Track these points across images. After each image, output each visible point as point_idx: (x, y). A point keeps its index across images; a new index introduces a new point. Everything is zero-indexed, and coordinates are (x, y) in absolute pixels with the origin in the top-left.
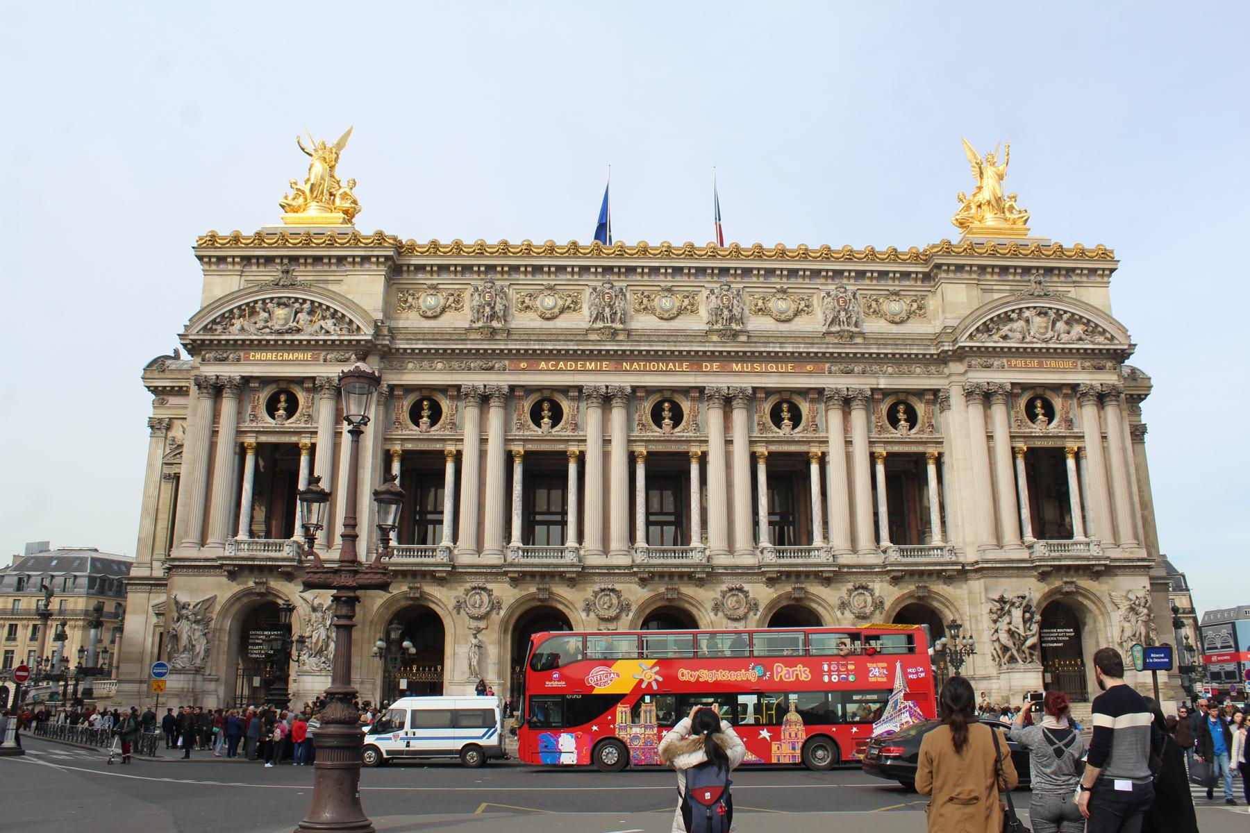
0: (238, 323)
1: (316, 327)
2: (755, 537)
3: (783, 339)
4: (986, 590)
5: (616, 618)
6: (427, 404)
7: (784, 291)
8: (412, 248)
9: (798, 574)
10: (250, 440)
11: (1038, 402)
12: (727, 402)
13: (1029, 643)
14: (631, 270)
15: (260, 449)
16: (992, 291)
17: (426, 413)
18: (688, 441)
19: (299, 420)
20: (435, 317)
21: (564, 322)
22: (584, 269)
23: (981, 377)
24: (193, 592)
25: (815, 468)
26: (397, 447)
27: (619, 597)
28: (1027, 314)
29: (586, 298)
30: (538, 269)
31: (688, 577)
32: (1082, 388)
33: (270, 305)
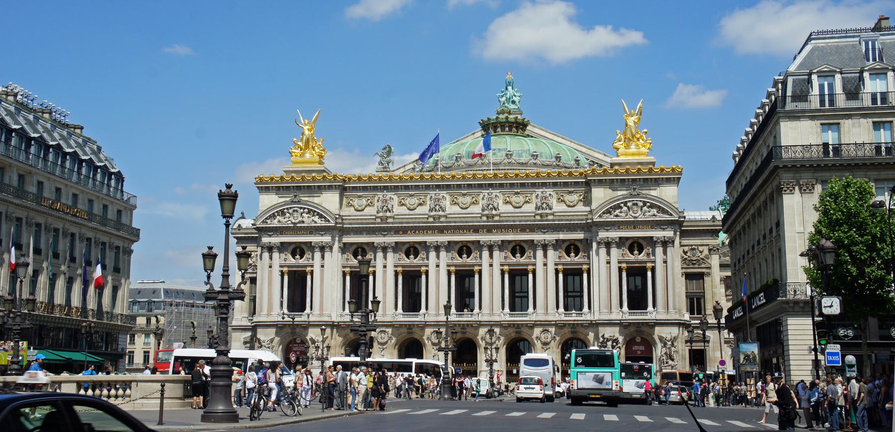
2: (503, 308)
6: (359, 250)
7: (517, 193)
8: (350, 179)
10: (285, 269)
11: (636, 245)
12: (491, 248)
14: (448, 187)
18: (473, 266)
20: (362, 210)
21: (419, 210)
22: (427, 187)
24: (266, 335)
26: (348, 270)
28: (629, 204)
30: (407, 188)
31: (469, 325)
32: (655, 239)
33: (291, 211)
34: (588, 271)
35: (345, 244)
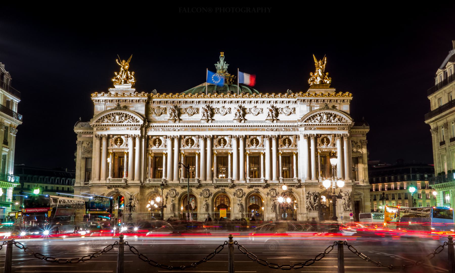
0: (106, 120)
1: (128, 121)
3: (253, 122)
4: (306, 191)
5: (208, 197)
9: (256, 186)
13: (315, 205)
15: (114, 154)
16: (314, 106)
17: (157, 142)
19: (123, 146)
23: (309, 132)
25: (262, 157)
27: (209, 192)
28: (322, 115)
29: (201, 110)
34: (297, 155)
35: (148, 136)
